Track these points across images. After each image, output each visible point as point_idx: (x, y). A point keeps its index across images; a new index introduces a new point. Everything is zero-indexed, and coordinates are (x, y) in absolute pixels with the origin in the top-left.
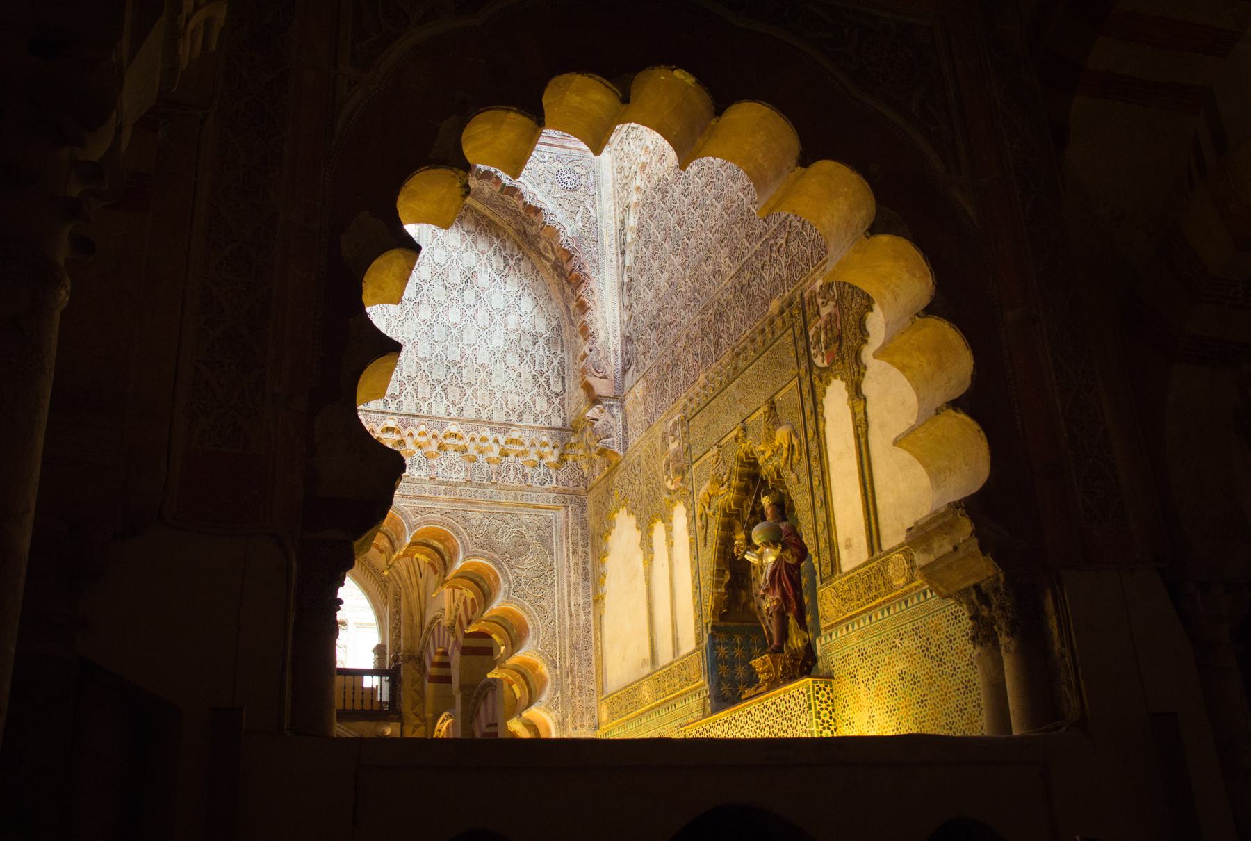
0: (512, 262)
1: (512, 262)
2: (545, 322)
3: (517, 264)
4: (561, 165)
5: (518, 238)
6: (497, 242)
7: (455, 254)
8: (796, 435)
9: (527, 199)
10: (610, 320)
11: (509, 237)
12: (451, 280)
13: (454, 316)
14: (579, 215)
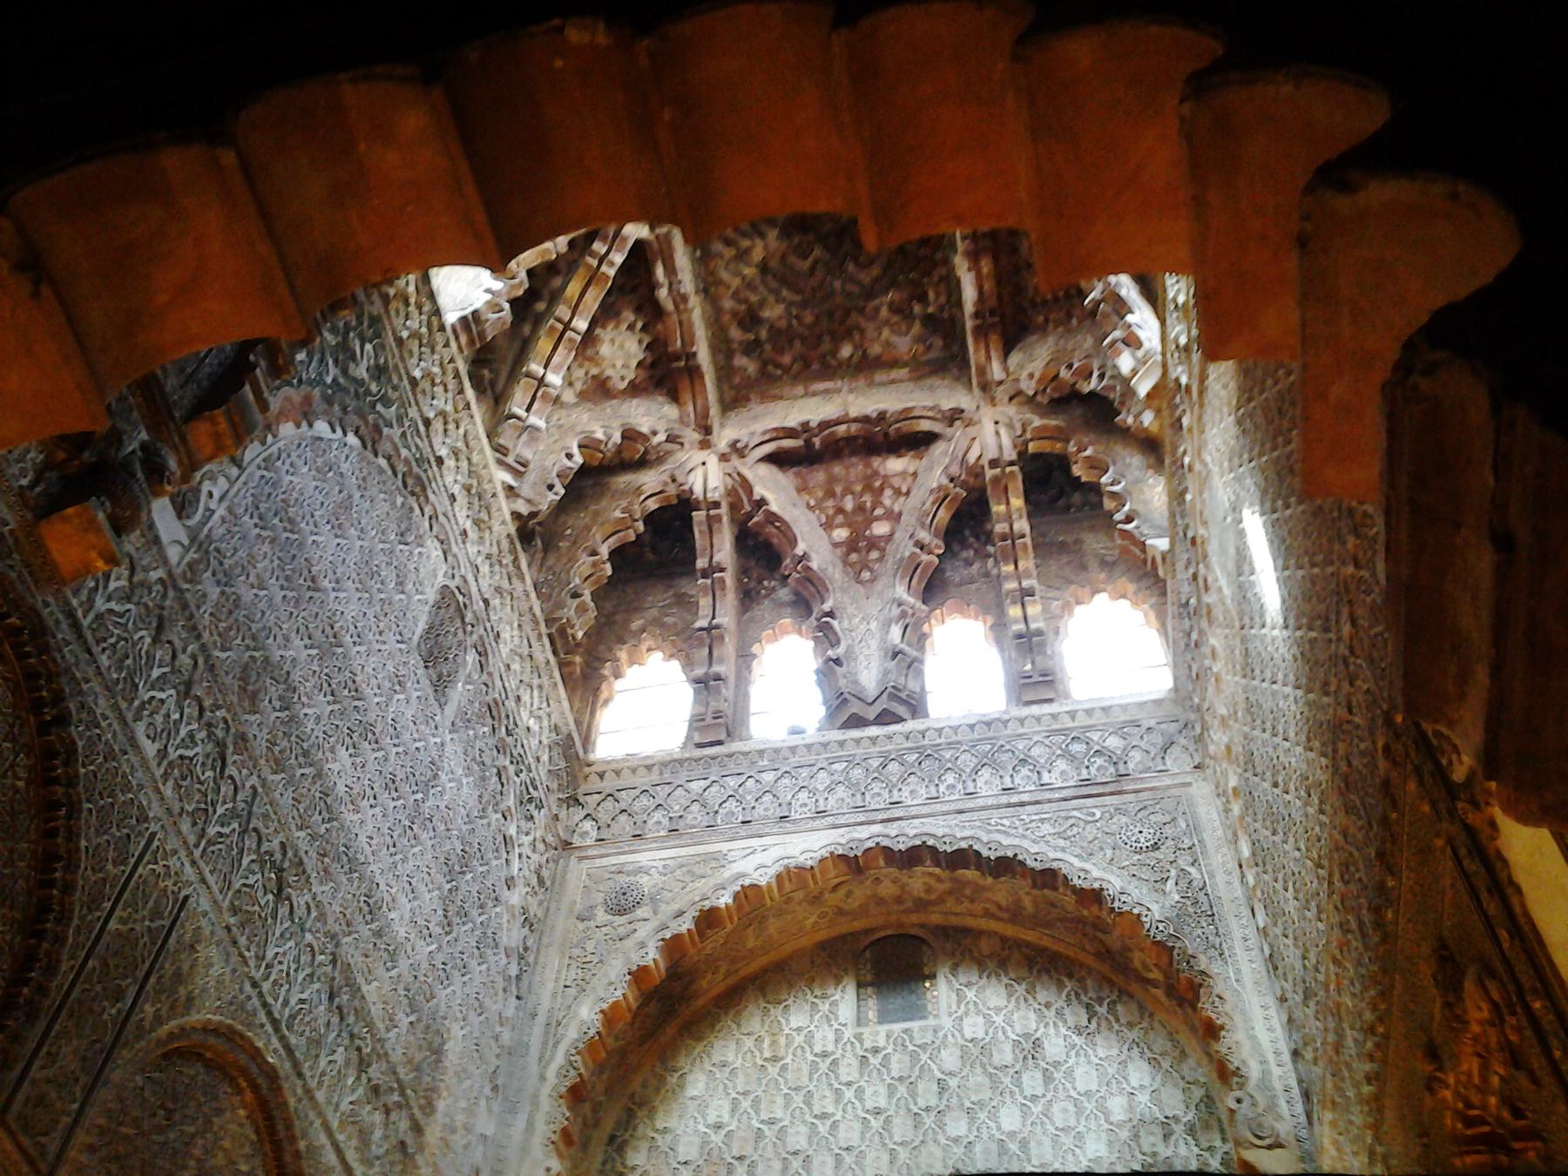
0: (1102, 1010)
1: (1102, 1010)
2: (1179, 1095)
3: (1111, 1010)
4: (1124, 819)
5: (1104, 968)
6: (1069, 985)
7: (999, 1020)
8: (1493, 975)
9: (1076, 882)
10: (1264, 1037)
11: (1090, 971)
12: (997, 1059)
13: (1010, 1119)
14: (1171, 883)
